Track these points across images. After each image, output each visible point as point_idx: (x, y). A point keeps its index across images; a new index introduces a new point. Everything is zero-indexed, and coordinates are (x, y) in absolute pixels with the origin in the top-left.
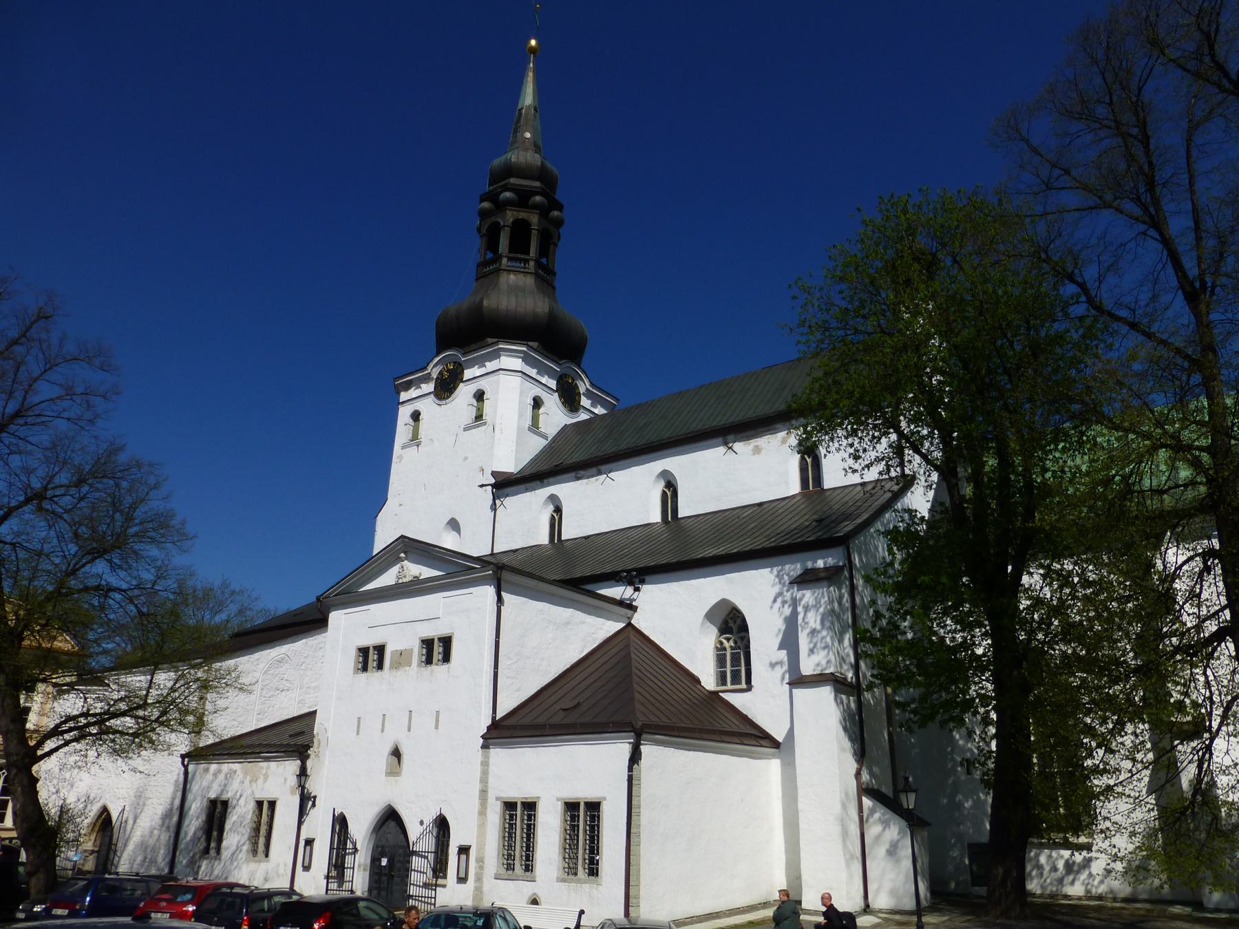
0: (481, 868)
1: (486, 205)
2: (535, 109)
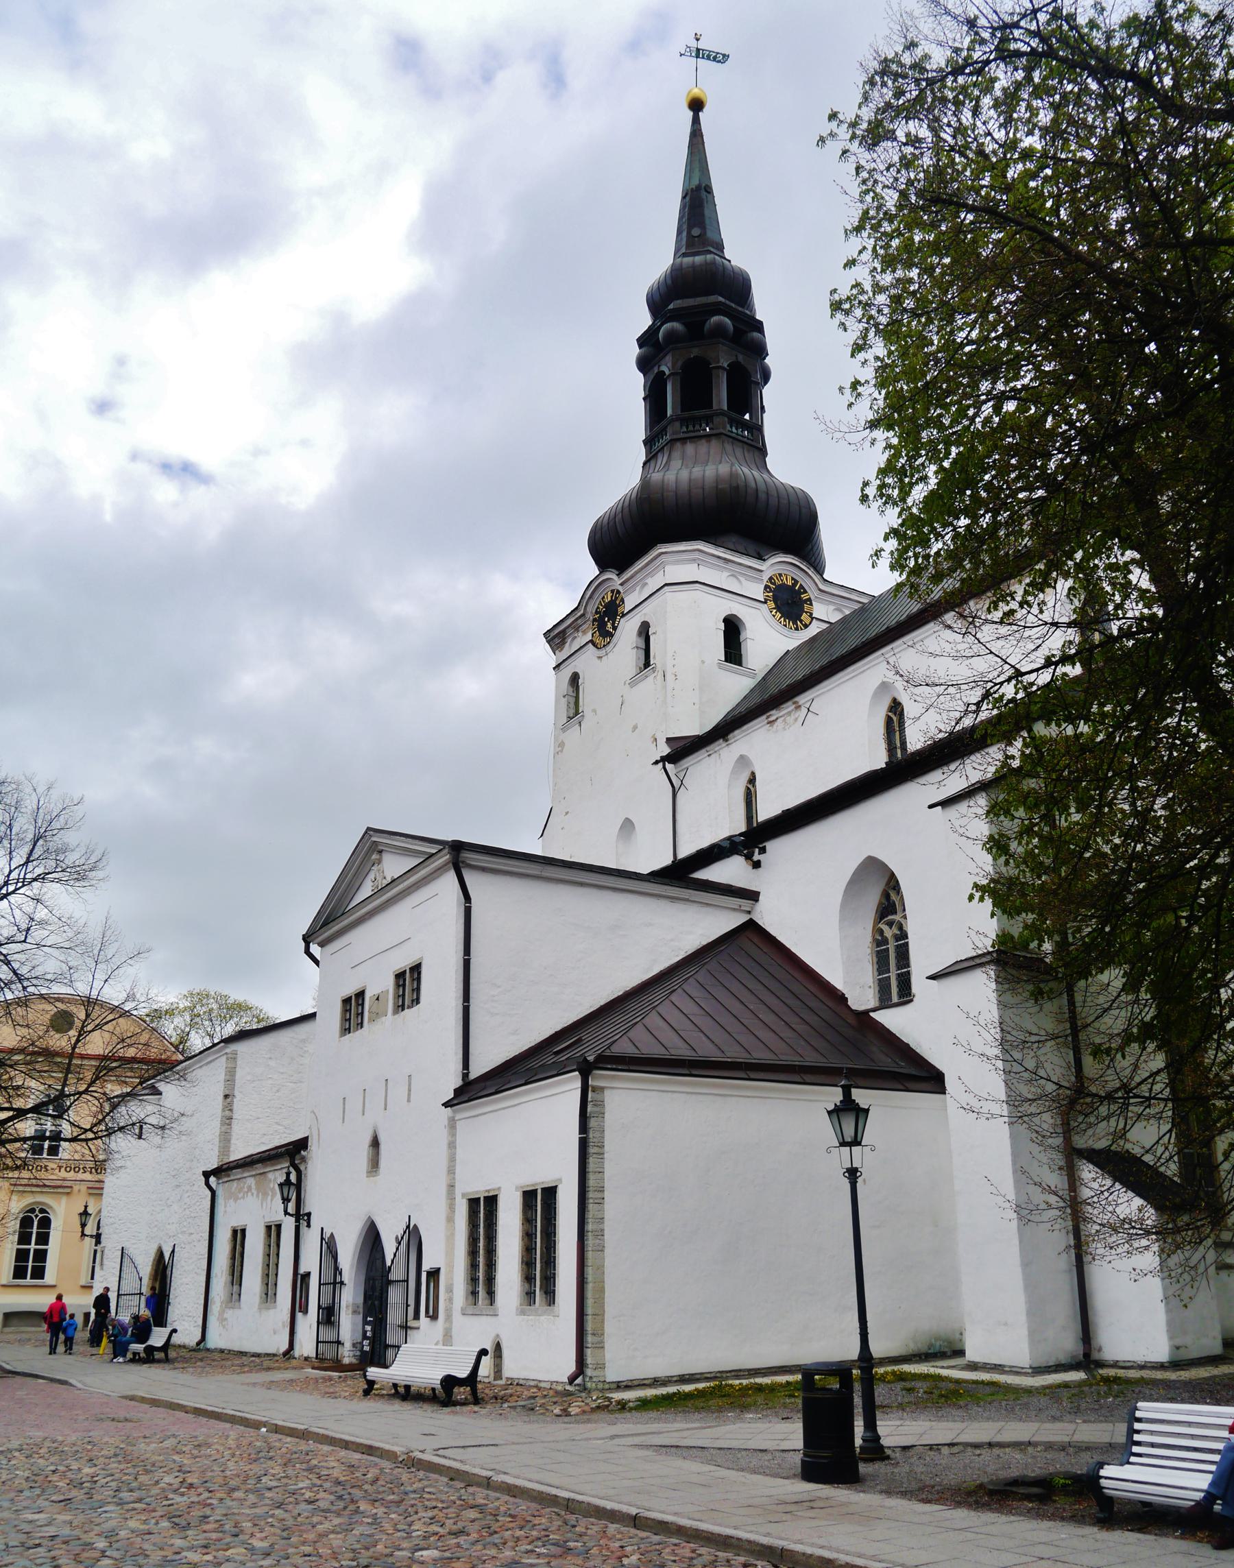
0: (450, 1300)
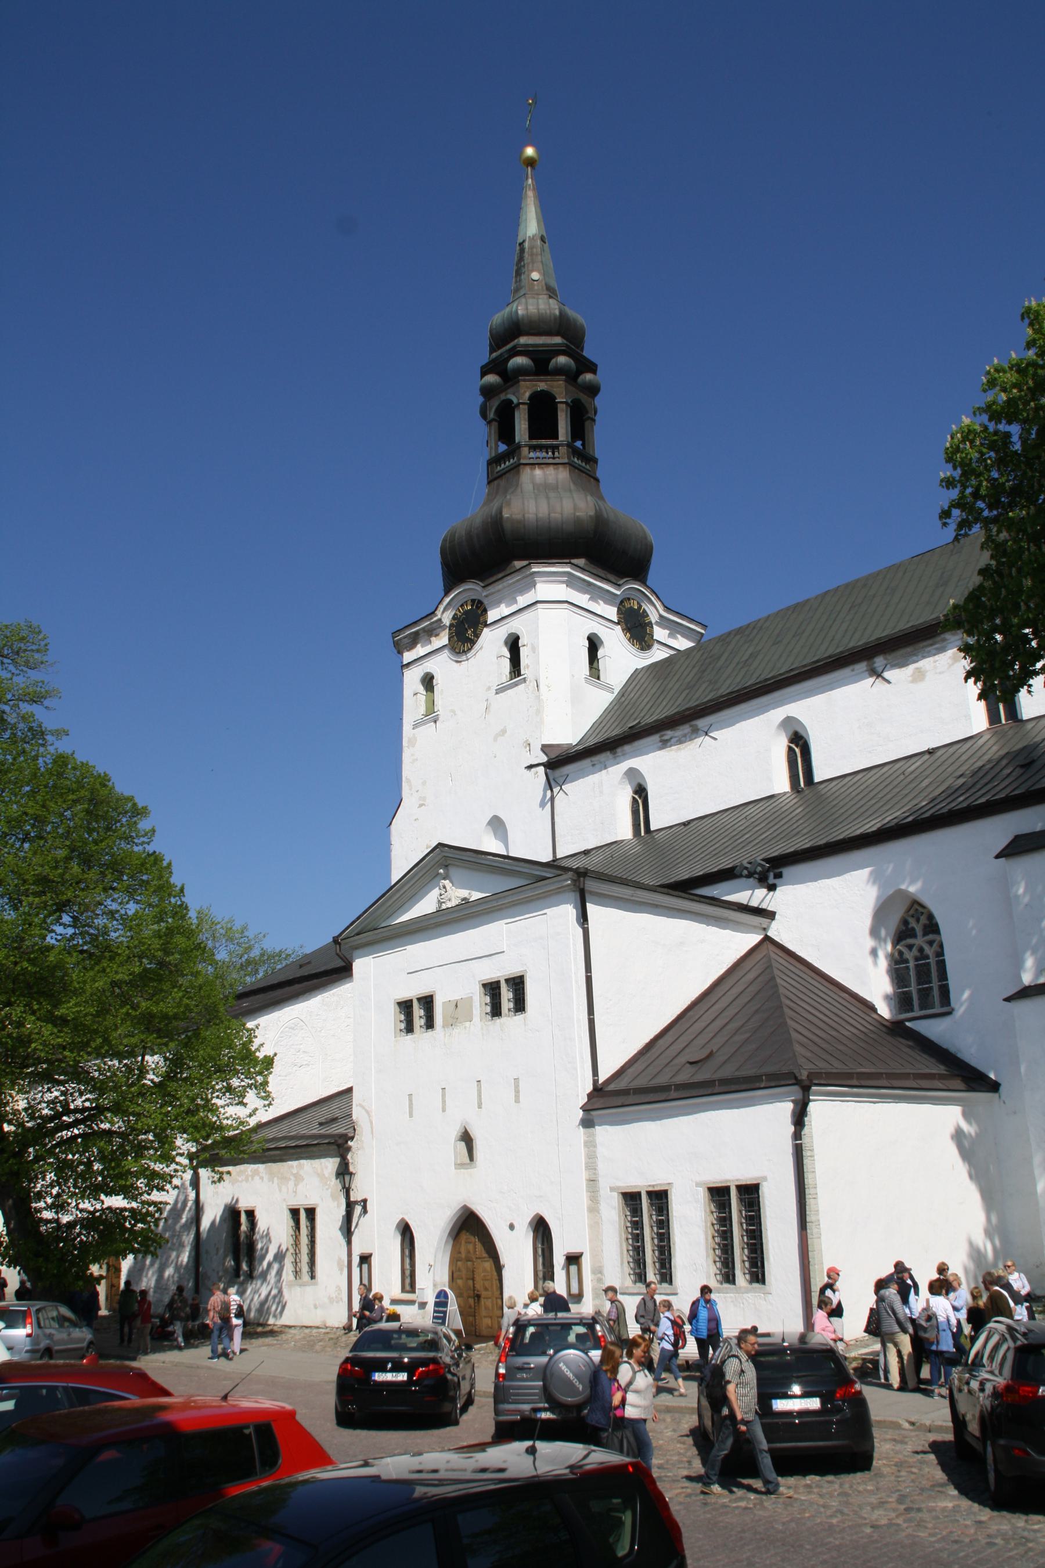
1: (492, 378)
2: (543, 239)
